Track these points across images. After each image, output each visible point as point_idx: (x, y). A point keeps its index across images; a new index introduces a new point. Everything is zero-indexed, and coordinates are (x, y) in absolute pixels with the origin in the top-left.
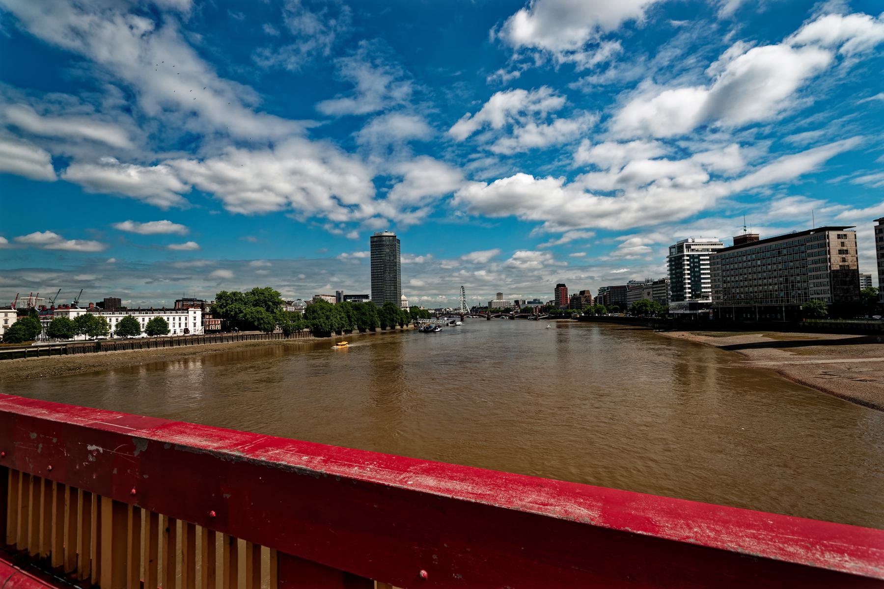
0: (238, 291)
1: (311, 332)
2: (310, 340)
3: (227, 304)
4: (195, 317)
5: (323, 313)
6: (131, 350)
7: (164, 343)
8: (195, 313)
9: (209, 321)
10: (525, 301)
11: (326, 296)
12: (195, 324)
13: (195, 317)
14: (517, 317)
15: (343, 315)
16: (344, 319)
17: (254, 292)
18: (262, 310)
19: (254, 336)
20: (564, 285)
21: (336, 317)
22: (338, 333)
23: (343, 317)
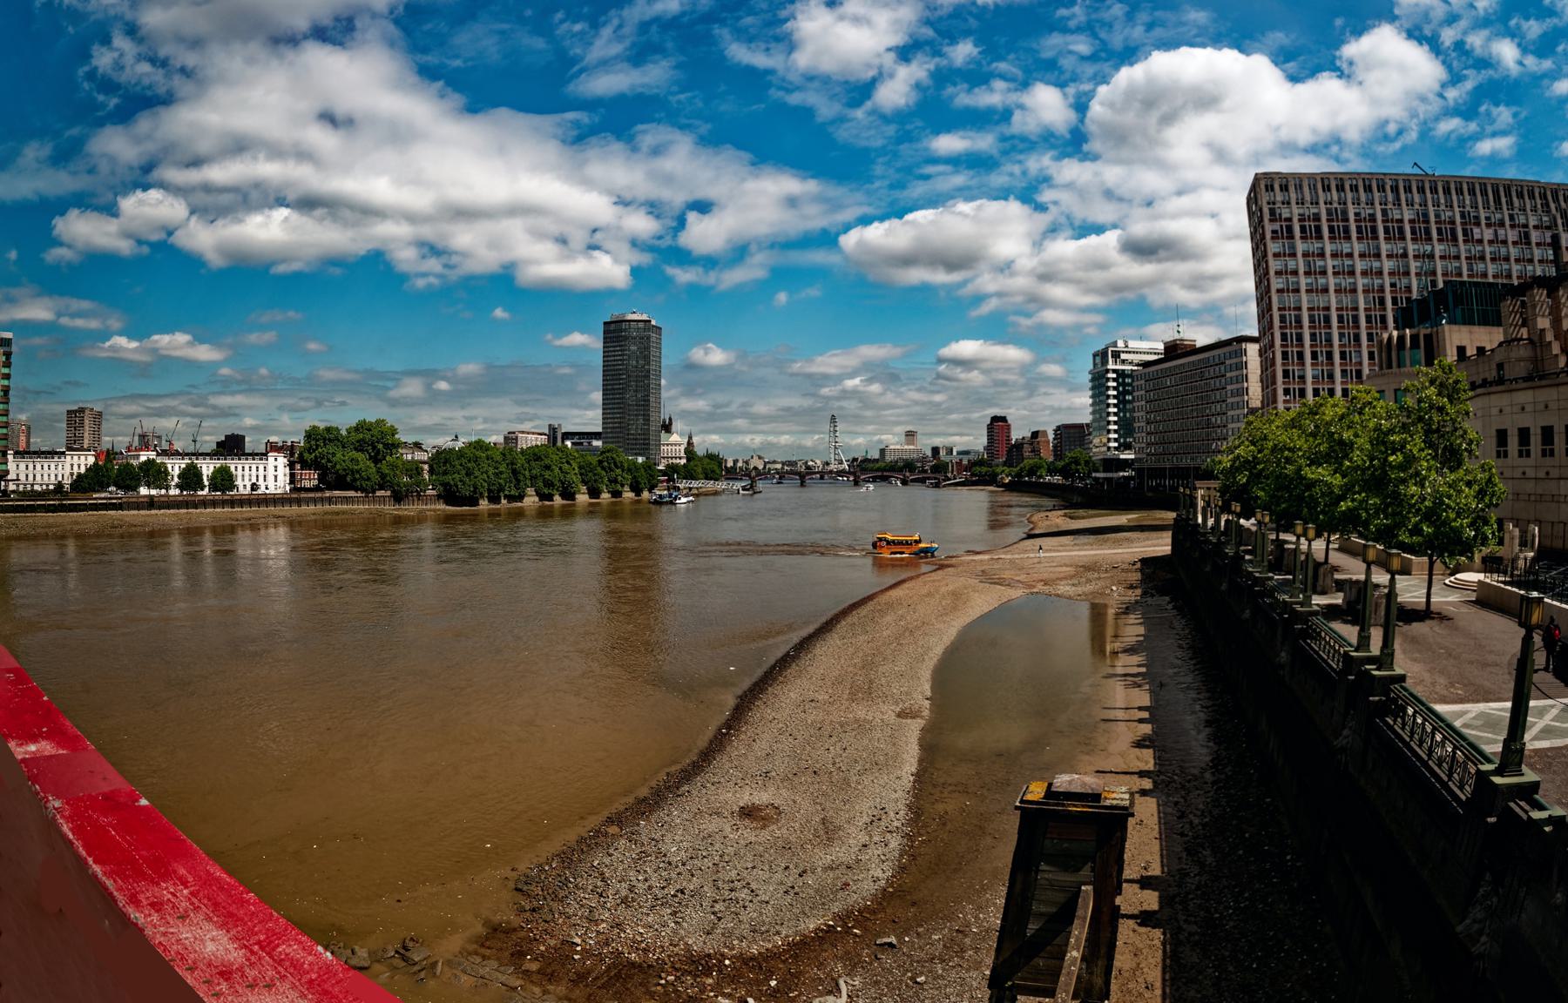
0: (334, 425)
1: (439, 497)
2: (439, 510)
3: (317, 446)
4: (276, 467)
5: (461, 465)
6: (186, 511)
7: (232, 503)
8: (276, 460)
9: (301, 474)
10: (952, 450)
11: (528, 433)
12: (276, 477)
13: (276, 467)
14: (913, 481)
15: (503, 468)
16: (504, 476)
17: (361, 427)
18: (360, 456)
19: (347, 500)
20: (1003, 419)
21: (486, 472)
22: (494, 499)
23: (501, 473)
